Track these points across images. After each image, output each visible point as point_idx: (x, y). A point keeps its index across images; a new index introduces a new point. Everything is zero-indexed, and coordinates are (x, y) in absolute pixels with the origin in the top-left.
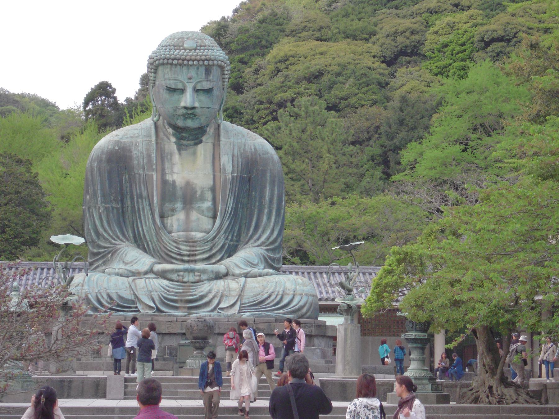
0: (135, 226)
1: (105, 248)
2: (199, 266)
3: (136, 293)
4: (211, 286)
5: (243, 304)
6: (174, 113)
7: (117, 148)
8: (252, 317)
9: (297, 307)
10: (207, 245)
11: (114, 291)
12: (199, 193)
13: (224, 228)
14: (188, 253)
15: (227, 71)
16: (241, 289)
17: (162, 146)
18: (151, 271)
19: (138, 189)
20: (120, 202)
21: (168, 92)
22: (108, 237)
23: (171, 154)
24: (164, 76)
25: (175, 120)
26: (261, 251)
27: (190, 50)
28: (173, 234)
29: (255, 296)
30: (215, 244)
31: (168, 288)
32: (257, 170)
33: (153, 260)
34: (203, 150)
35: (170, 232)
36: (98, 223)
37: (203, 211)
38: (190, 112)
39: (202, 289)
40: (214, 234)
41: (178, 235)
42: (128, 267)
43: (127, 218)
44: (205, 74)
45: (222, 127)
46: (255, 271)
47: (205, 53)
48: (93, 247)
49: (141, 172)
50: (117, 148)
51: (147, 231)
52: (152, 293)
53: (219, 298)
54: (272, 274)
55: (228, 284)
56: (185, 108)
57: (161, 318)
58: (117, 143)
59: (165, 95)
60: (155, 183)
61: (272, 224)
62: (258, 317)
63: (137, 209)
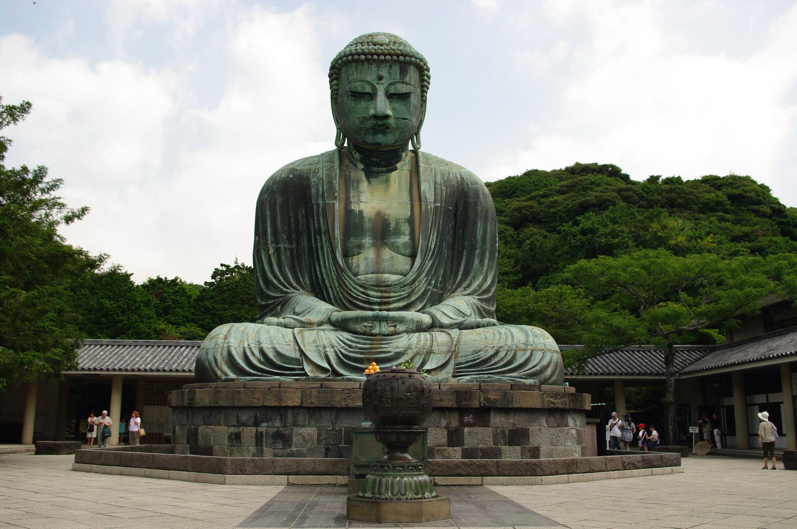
5: (458, 364)
7: (291, 176)
8: (475, 383)
9: (538, 368)
10: (404, 290)
11: (270, 346)
12: (392, 226)
13: (426, 270)
16: (455, 343)
18: (329, 322)
19: (316, 222)
20: (294, 242)
21: (353, 98)
25: (363, 135)
26: (474, 300)
27: (381, 45)
28: (359, 277)
29: (476, 352)
30: (414, 289)
31: (349, 343)
33: (330, 307)
34: (399, 176)
35: (356, 275)
38: (380, 123)
39: (400, 345)
40: (413, 277)
44: (400, 74)
48: (262, 300)
49: (321, 202)
50: (291, 176)
52: (328, 349)
53: (423, 356)
54: (494, 325)
55: (436, 337)
56: (375, 117)
57: (337, 385)
60: (337, 213)
61: (485, 268)
62: (484, 382)
63: (314, 249)
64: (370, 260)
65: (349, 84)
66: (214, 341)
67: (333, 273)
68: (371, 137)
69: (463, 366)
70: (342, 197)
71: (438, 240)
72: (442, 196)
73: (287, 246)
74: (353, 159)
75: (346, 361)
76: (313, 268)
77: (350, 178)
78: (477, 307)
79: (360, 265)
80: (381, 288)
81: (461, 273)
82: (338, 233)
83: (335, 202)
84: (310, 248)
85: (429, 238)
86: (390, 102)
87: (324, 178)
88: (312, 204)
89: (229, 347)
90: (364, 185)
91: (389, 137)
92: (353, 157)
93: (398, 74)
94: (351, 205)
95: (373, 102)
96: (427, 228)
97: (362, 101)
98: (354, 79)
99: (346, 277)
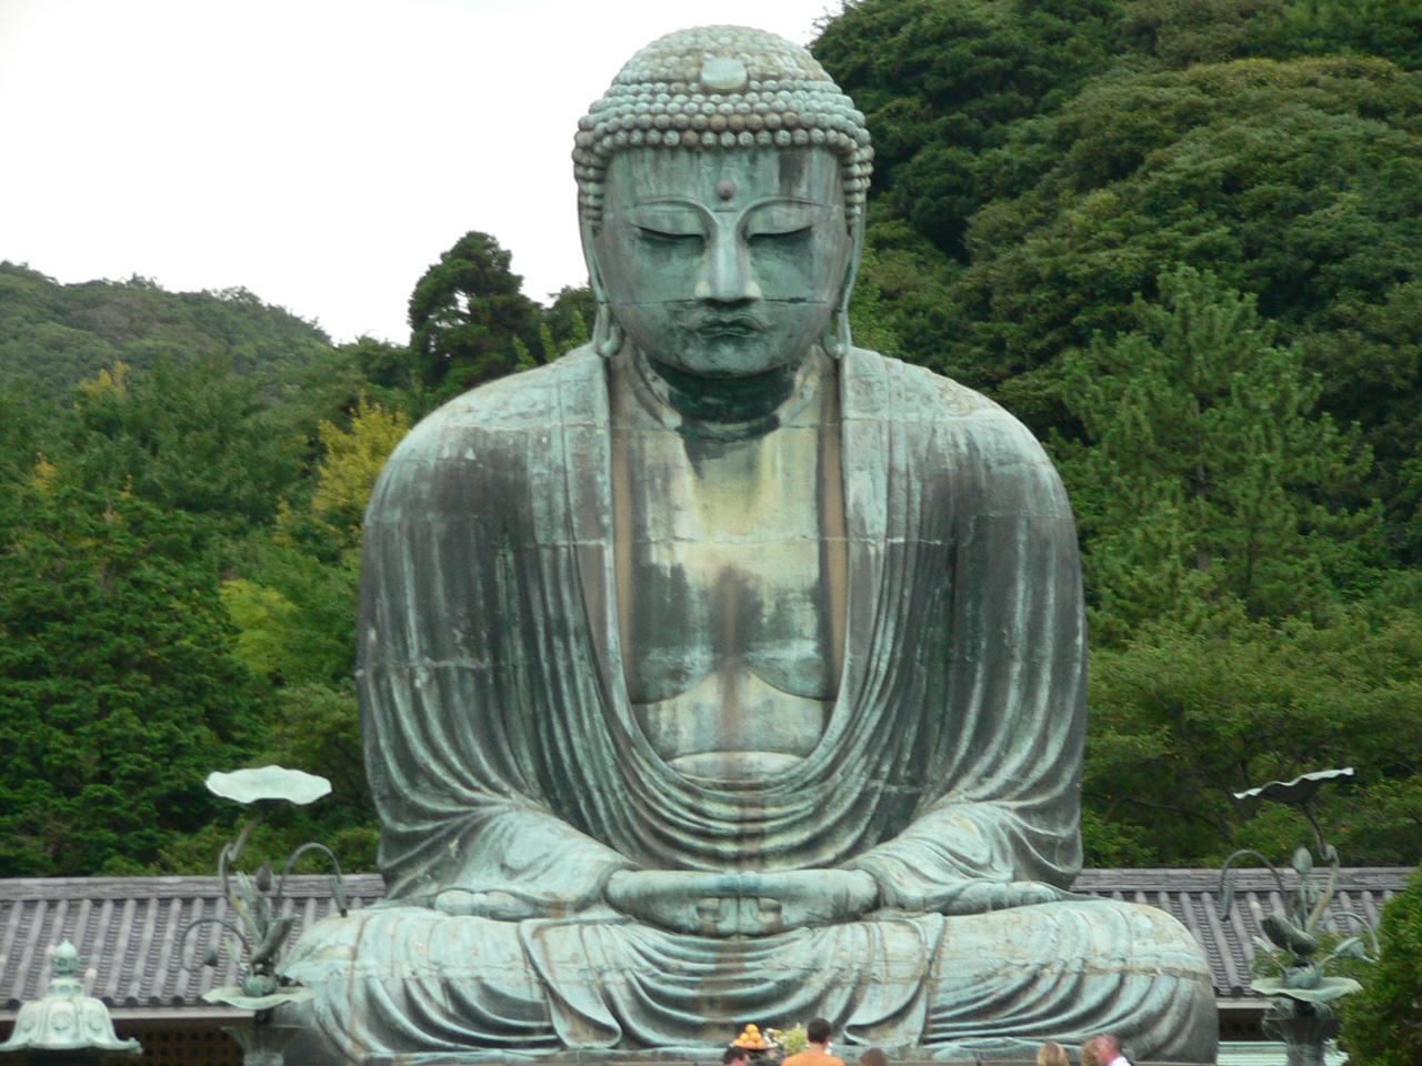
0: (544, 735)
1: (436, 816)
2: (775, 876)
3: (547, 976)
4: (820, 947)
6: (675, 325)
7: (470, 455)
9: (1135, 1018)
10: (803, 799)
11: (467, 973)
12: (769, 610)
13: (865, 737)
14: (734, 828)
15: (861, 163)
16: (928, 955)
17: (634, 443)
18: (603, 897)
19: (550, 599)
20: (486, 652)
21: (648, 247)
22: (448, 779)
23: (667, 473)
24: (632, 190)
26: (1004, 814)
27: (725, 93)
28: (678, 762)
30: (832, 794)
32: (981, 522)
33: (607, 856)
34: (785, 451)
35: (668, 755)
36: (409, 727)
37: (785, 674)
38: (727, 317)
39: (790, 960)
40: (829, 759)
41: (697, 765)
42: (517, 886)
43: (513, 704)
44: (782, 178)
45: (847, 369)
46: (979, 888)
47: (780, 104)
48: (397, 818)
49: (562, 542)
50: (470, 455)
51: (588, 752)
52: (608, 977)
53: (849, 990)
54: (1040, 900)
55: (882, 939)
56: (712, 303)
58: (473, 436)
60: (609, 577)
61: (1039, 717)
64: (706, 711)
65: (636, 205)
66: (325, 963)
67: (605, 751)
68: (701, 353)
69: (948, 1014)
70: (624, 523)
71: (900, 646)
72: (909, 512)
73: (468, 662)
74: (647, 395)
75: (653, 1006)
76: (543, 726)
77: (642, 461)
78: (1013, 837)
79: (683, 729)
80: (741, 794)
81: (967, 733)
82: (613, 637)
83: (603, 542)
84: (534, 669)
85: (873, 644)
86: (755, 255)
87: (570, 467)
88: (537, 549)
89: (366, 980)
90: (685, 484)
91: (753, 352)
92: (648, 386)
93: (776, 182)
94: (648, 552)
95: (705, 257)
96: (867, 615)
97: (674, 255)
98: (651, 196)
99: (643, 763)
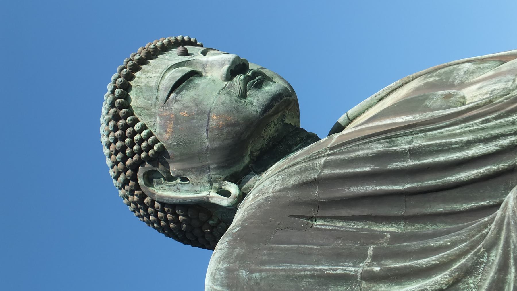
1: (503, 268)
21: (184, 91)
49: (322, 161)
59: (187, 96)
65: (158, 89)
79: (492, 89)
